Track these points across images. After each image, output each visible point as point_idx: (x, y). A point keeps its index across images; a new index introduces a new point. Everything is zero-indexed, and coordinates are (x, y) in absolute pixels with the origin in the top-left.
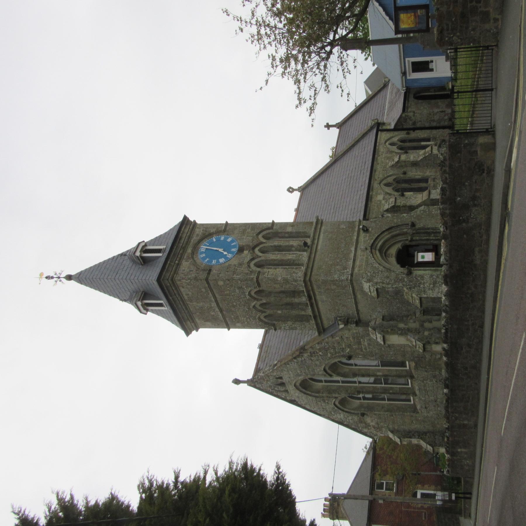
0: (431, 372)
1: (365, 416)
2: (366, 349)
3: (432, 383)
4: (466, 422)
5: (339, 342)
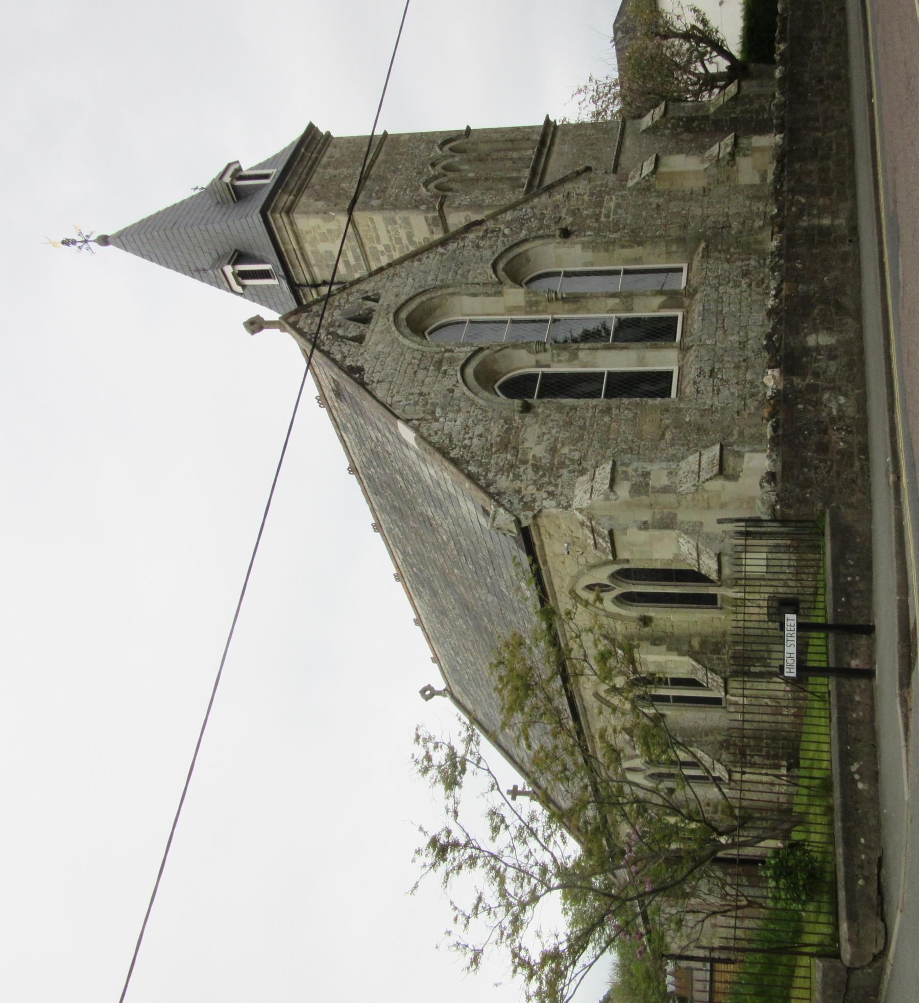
0: (739, 263)
1: (529, 418)
2: (607, 216)
3: (738, 290)
4: (826, 222)
5: (558, 206)
